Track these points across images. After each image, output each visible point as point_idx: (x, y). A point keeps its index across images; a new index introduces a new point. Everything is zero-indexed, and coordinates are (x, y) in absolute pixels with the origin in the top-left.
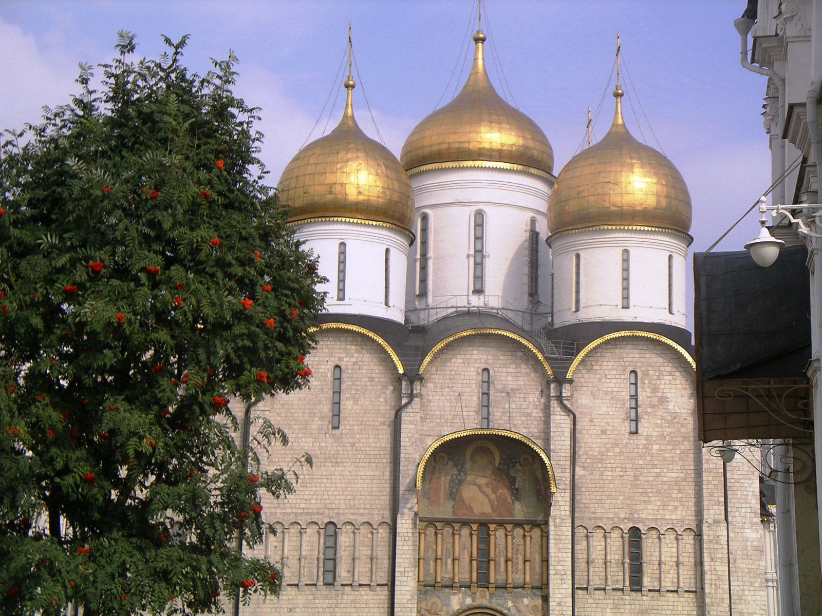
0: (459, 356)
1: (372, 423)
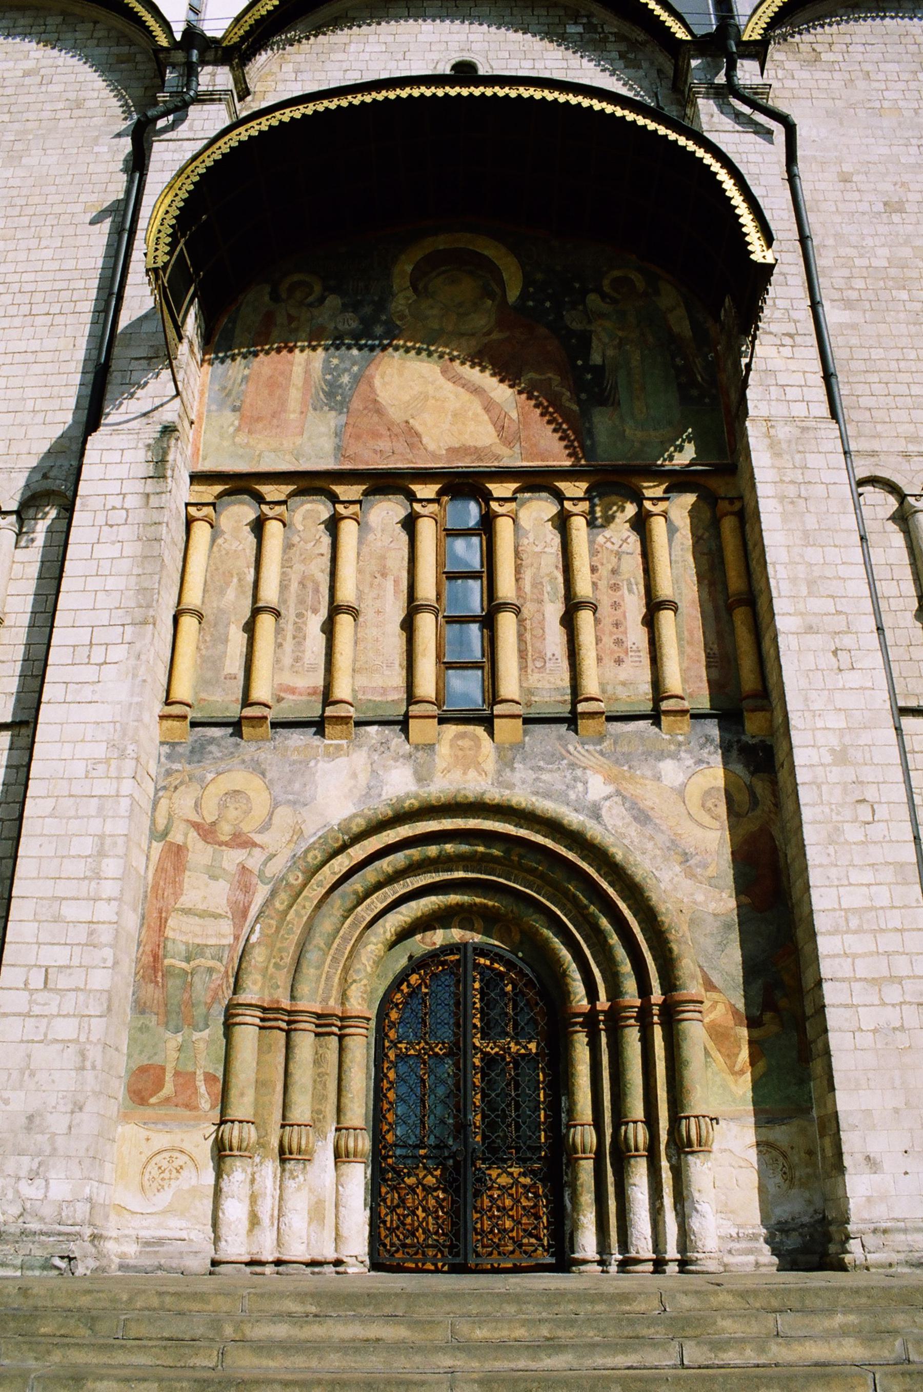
0: (372, 39)
1: (57, 209)
